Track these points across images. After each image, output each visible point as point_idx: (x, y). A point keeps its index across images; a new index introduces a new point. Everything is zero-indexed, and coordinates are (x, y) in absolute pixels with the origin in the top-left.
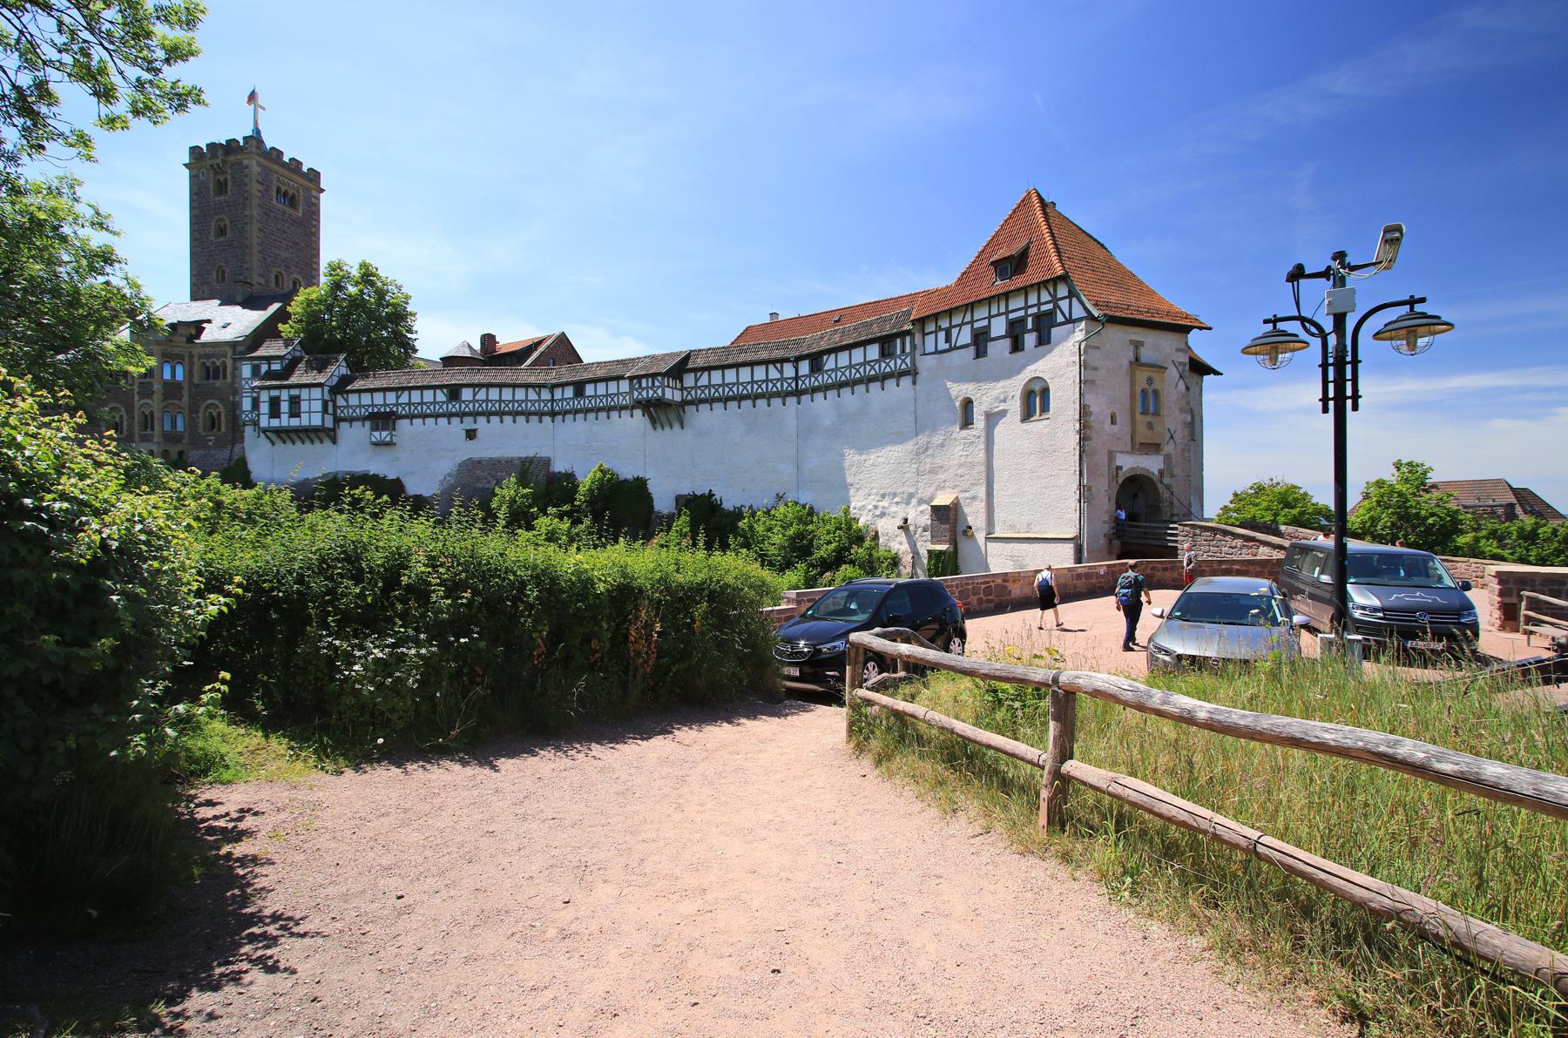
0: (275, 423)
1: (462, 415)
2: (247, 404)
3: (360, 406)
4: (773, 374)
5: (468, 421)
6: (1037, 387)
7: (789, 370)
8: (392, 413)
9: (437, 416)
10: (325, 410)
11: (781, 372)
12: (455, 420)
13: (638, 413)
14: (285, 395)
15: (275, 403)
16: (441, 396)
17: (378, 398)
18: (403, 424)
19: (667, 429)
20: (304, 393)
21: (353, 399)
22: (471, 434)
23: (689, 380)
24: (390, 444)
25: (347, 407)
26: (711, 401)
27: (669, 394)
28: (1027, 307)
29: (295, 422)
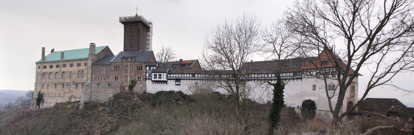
0: (155, 80)
1: (195, 79)
2: (147, 75)
3: (173, 77)
6: (331, 85)
7: (270, 76)
9: (189, 79)
12: (194, 81)
14: (158, 74)
15: (155, 76)
16: (191, 76)
17: (177, 76)
18: (182, 81)
20: (162, 74)
21: (172, 75)
24: (180, 85)
25: (170, 77)
28: (330, 70)
29: (160, 80)
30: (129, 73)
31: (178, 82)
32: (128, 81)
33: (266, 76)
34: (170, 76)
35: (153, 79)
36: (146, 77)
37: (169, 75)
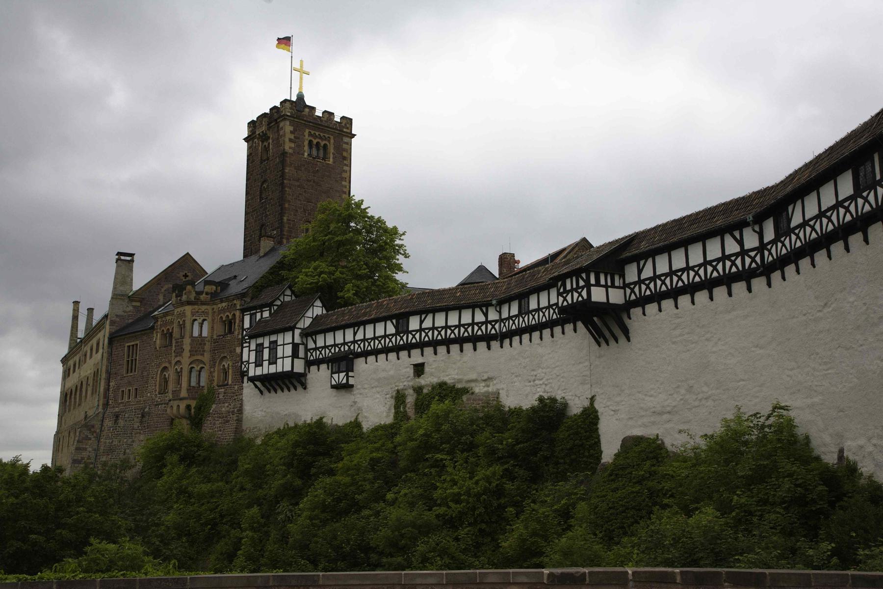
0: (259, 372)
1: (409, 347)
4: (732, 247)
5: (416, 352)
8: (351, 352)
9: (386, 350)
10: (295, 355)
11: (741, 242)
12: (403, 354)
13: (580, 325)
15: (260, 349)
16: (391, 330)
18: (359, 363)
19: (612, 342)
22: (419, 369)
23: (631, 274)
25: (316, 349)
26: (658, 298)
27: (598, 295)
29: (273, 369)
30: (186, 353)
31: (339, 372)
32: (184, 393)
33: (732, 247)
34: (315, 342)
35: (251, 374)
36: (242, 363)
37: (310, 340)
